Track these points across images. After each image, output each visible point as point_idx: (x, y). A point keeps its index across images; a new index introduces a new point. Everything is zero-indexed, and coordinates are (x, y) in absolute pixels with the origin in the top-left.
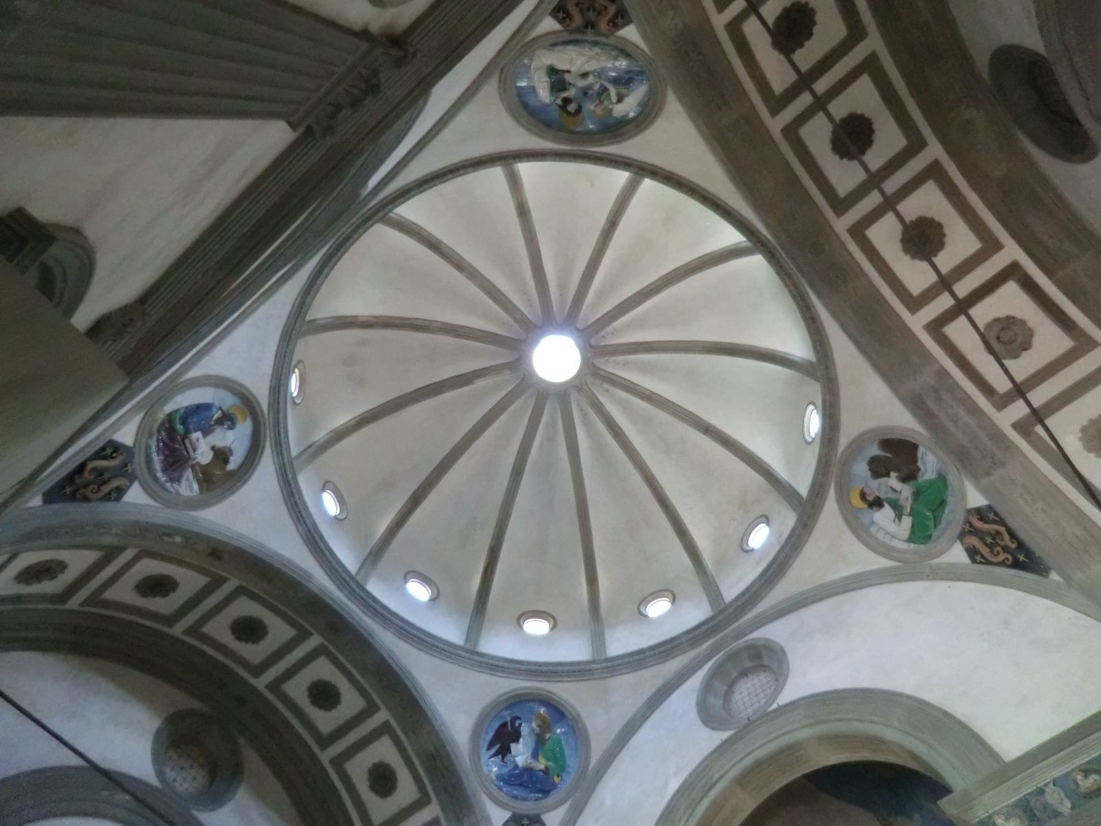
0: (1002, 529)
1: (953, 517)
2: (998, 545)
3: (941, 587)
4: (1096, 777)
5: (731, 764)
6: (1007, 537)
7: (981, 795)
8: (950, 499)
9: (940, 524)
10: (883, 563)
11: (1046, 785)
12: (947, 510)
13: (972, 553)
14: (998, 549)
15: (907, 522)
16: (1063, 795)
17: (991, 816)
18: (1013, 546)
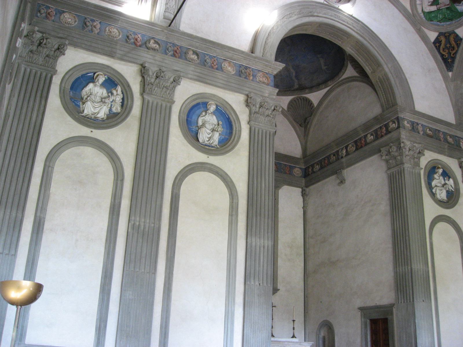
0: (456, 49)
1: (446, 27)
2: (449, 51)
3: (417, 37)
4: (431, 133)
5: (324, 16)
6: (454, 52)
7: (408, 112)
8: (454, 22)
9: (441, 23)
10: (408, 7)
11: (420, 124)
12: (448, 23)
13: (437, 42)
14: (447, 51)
15: (434, 8)
17: (403, 118)
18: (452, 55)
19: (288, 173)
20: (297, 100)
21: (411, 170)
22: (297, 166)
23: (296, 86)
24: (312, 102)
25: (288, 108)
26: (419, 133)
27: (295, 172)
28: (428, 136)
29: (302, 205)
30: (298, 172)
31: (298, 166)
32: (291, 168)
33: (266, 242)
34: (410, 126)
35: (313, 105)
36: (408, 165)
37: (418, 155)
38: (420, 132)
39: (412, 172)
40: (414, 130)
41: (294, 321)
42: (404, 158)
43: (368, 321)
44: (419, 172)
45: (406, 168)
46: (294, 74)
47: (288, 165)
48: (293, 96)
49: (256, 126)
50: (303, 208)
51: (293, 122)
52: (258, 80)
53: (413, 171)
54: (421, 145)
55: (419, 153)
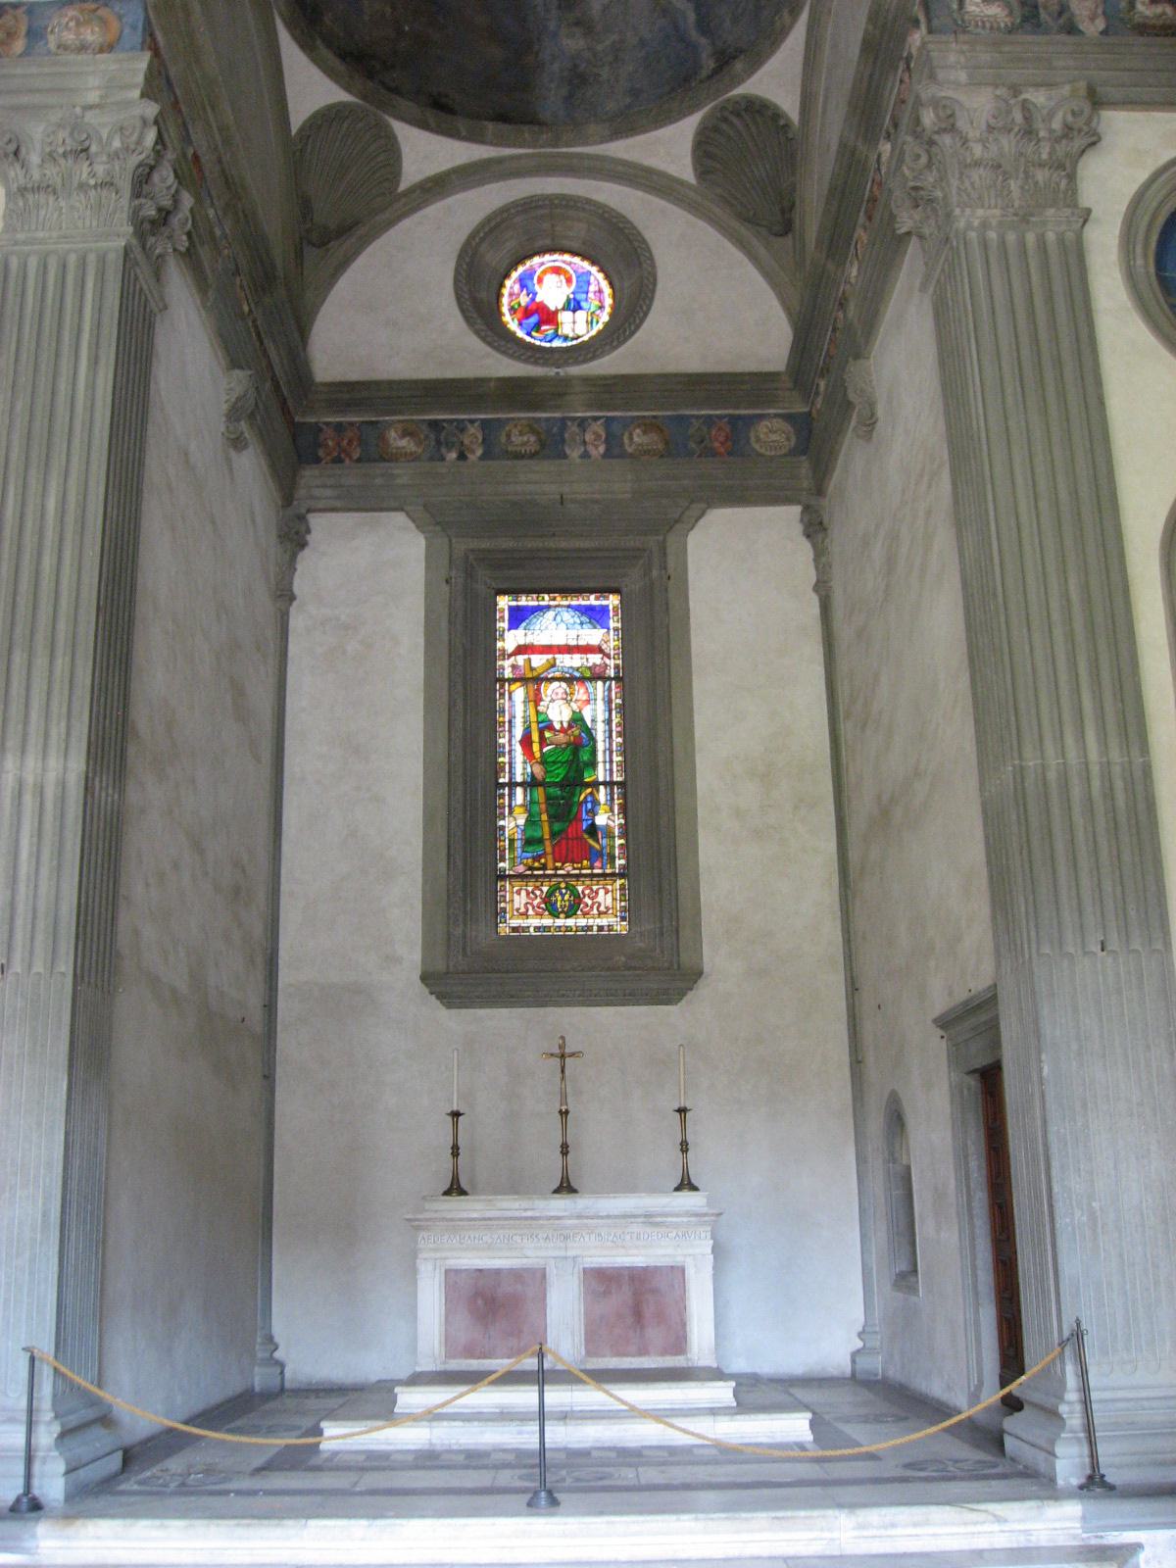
16: (1100, 11)
19: (722, 450)
20: (724, 126)
21: (1011, 237)
22: (772, 411)
23: (709, 64)
24: (776, 107)
25: (702, 172)
26: (1071, 29)
27: (758, 440)
28: (1143, 29)
29: (812, 576)
30: (774, 437)
31: (774, 408)
32: (739, 427)
33: (54, 763)
34: (1011, 13)
35: (788, 119)
36: (980, 212)
37: (1061, 149)
38: (1084, 26)
39: (1022, 244)
40: (1038, 25)
41: (682, 1111)
42: (955, 182)
43: (973, 1082)
44: (1070, 236)
45: (973, 235)
46: (692, 17)
47: (720, 417)
48: (699, 110)
49: (27, 248)
50: (816, 588)
51: (735, 224)
52: (52, 46)
53: (1030, 238)
54: (1066, 90)
55: (1068, 130)
